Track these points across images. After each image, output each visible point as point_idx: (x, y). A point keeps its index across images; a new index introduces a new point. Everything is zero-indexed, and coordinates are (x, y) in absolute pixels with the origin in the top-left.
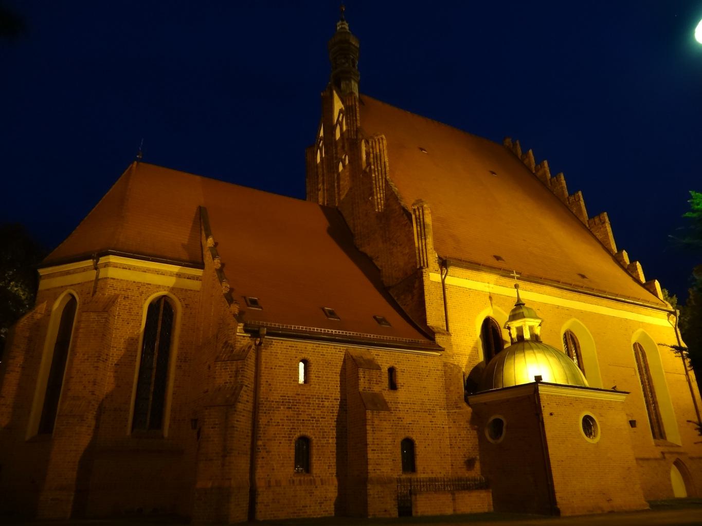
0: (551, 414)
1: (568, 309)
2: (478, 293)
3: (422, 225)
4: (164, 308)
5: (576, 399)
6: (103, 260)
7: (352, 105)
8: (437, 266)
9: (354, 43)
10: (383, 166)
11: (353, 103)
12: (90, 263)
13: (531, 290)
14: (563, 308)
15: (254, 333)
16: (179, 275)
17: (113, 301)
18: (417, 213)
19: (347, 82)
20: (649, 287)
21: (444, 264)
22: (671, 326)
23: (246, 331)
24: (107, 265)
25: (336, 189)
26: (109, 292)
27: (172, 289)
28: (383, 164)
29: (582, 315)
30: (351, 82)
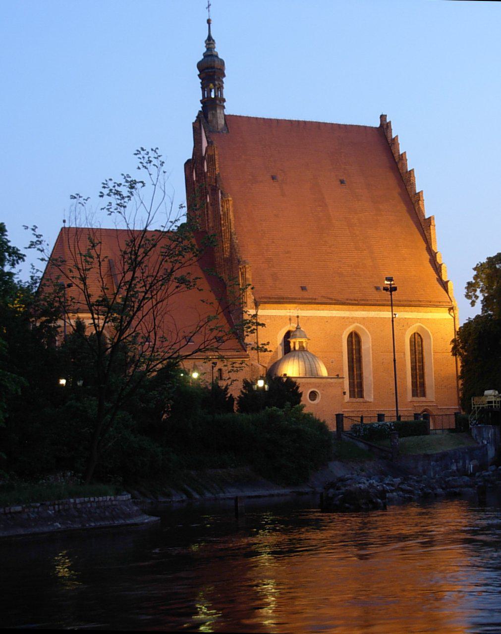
1: (352, 318)
2: (281, 317)
5: (308, 383)
7: (212, 155)
8: (253, 305)
10: (229, 222)
11: (213, 152)
13: (323, 310)
14: (348, 318)
18: (242, 270)
19: (214, 112)
21: (257, 305)
22: (451, 317)
25: (206, 216)
28: (229, 220)
29: (363, 320)
30: (216, 111)
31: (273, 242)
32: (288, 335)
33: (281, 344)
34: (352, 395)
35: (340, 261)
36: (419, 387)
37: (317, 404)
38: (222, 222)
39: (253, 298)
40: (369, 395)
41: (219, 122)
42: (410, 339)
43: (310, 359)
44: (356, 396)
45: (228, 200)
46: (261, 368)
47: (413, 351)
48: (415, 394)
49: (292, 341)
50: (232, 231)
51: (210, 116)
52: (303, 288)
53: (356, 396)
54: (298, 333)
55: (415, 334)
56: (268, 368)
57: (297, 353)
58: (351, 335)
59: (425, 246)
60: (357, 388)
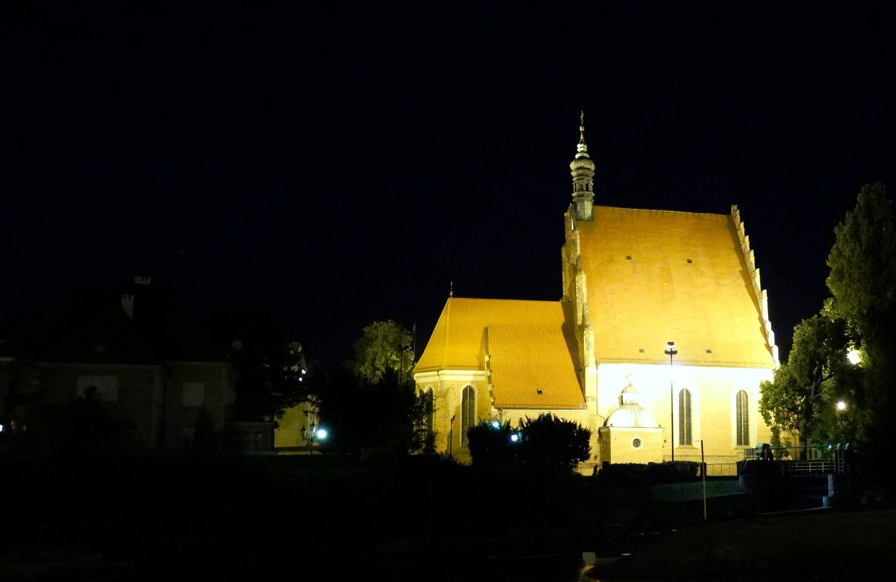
0: (615, 439)
3: (588, 344)
4: (470, 390)
5: (632, 432)
6: (440, 372)
9: (587, 167)
12: (435, 373)
15: (499, 409)
16: (474, 375)
17: (447, 391)
19: (582, 204)
20: (769, 349)
23: (496, 408)
24: (443, 374)
26: (445, 387)
27: (472, 382)
30: (584, 203)
31: (620, 312)
32: (622, 392)
33: (618, 398)
34: (682, 442)
35: (677, 328)
36: (743, 437)
37: (640, 451)
38: (577, 295)
39: (595, 359)
40: (696, 444)
41: (586, 212)
42: (737, 397)
43: (637, 411)
44: (685, 443)
45: (582, 277)
46: (598, 418)
47: (739, 407)
48: (739, 442)
49: (623, 395)
50: (584, 302)
51: (579, 208)
52: (642, 351)
53: (685, 443)
54: (628, 389)
55: (741, 391)
56: (606, 419)
57: (626, 406)
58: (683, 390)
59: (757, 315)
60: (686, 438)
